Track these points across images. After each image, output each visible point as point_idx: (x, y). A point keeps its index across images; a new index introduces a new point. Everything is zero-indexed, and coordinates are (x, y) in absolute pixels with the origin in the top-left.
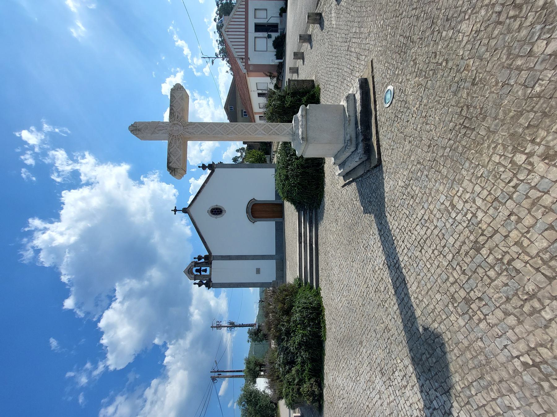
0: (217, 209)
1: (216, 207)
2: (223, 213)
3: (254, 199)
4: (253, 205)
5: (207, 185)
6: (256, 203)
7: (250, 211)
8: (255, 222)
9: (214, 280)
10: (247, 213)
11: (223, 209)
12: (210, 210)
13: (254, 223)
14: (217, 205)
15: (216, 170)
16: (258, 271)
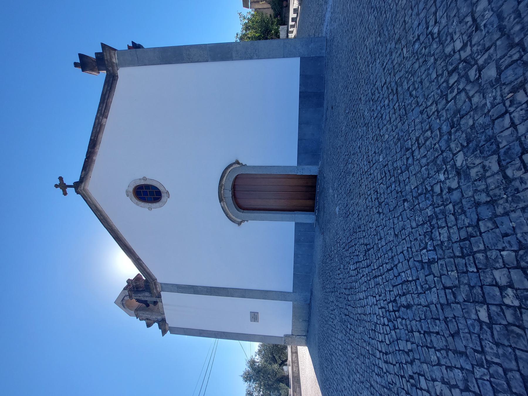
0: (148, 187)
1: (143, 183)
2: (163, 199)
3: (237, 162)
4: (236, 178)
5: (109, 123)
6: (243, 172)
7: (229, 194)
8: (241, 222)
9: (170, 322)
10: (221, 200)
11: (161, 189)
12: (131, 189)
13: (239, 224)
14: (145, 179)
15: (123, 73)
16: (254, 317)
